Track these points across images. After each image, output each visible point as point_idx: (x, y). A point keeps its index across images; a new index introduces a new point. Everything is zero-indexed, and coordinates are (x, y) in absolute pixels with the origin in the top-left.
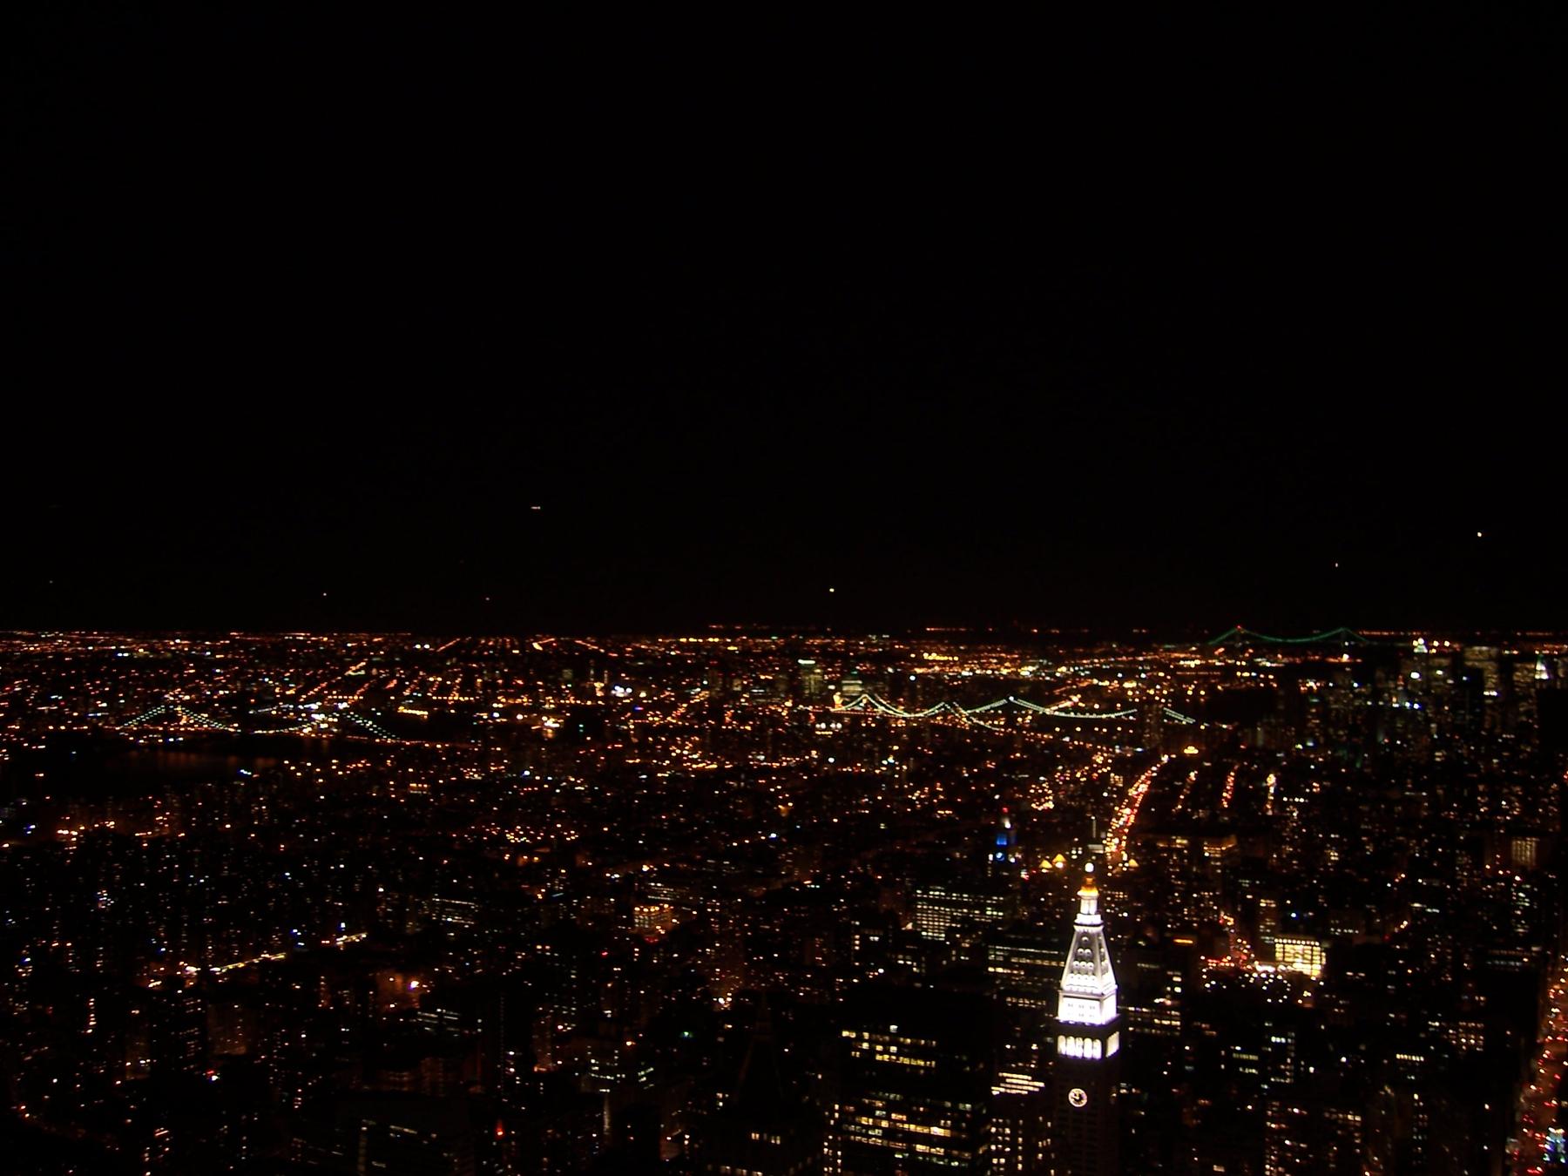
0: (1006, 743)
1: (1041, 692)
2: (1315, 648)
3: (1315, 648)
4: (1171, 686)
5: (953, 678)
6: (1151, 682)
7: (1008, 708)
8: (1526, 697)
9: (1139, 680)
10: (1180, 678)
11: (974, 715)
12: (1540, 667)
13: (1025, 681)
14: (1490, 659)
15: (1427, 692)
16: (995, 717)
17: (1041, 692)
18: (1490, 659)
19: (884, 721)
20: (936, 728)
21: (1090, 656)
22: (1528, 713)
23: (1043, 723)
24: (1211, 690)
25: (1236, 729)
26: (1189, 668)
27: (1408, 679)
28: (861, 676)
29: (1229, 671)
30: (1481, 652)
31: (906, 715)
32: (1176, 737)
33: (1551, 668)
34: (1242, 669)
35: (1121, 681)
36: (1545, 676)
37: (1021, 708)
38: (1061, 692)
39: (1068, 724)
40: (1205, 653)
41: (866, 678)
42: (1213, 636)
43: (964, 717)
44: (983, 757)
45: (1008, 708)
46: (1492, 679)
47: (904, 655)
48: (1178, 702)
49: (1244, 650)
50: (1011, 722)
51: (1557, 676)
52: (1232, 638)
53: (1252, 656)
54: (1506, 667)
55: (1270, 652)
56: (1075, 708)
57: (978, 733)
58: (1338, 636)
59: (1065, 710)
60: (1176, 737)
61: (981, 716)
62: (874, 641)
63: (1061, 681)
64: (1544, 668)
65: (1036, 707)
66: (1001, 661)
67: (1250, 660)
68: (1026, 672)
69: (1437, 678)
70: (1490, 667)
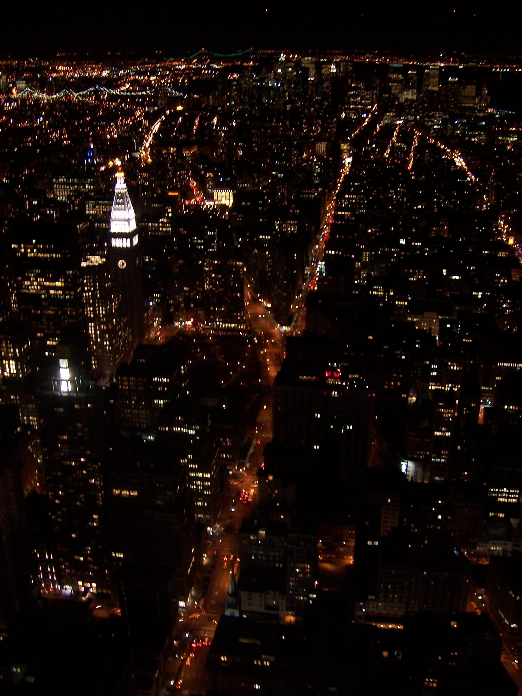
0: (96, 108)
1: (112, 83)
2: (238, 58)
3: (238, 58)
4: (172, 78)
5: (70, 79)
6: (163, 76)
7: (96, 92)
8: (326, 81)
9: (157, 76)
10: (176, 74)
11: (80, 95)
12: (333, 67)
13: (104, 78)
14: (312, 63)
15: (284, 78)
16: (90, 96)
17: (112, 83)
18: (312, 63)
19: (37, 101)
20: (61, 103)
21: (135, 65)
22: (327, 88)
23: (113, 98)
24: (190, 79)
25: (200, 98)
26: (180, 70)
27: (276, 73)
28: (25, 79)
29: (198, 71)
30: (308, 60)
31: (48, 97)
32: (173, 101)
33: (338, 67)
34: (205, 70)
35: (149, 77)
36: (335, 71)
37: (101, 92)
38: (121, 83)
39: (124, 98)
40: (188, 62)
41: (28, 80)
42: (191, 54)
43: (75, 96)
44: (85, 115)
45: (96, 92)
46: (313, 72)
47: (47, 68)
48: (175, 86)
49: (205, 60)
50: (98, 98)
51: (340, 71)
52: (201, 54)
53: (209, 63)
54: (319, 66)
55: (217, 61)
56: (128, 90)
57: (82, 104)
58: (248, 53)
59: (123, 91)
60: (173, 101)
61: (83, 96)
62: (32, 62)
63: (120, 78)
64: (334, 67)
65: (107, 90)
66: (93, 69)
67: (209, 65)
68: (104, 74)
69: (289, 72)
70: (312, 66)
